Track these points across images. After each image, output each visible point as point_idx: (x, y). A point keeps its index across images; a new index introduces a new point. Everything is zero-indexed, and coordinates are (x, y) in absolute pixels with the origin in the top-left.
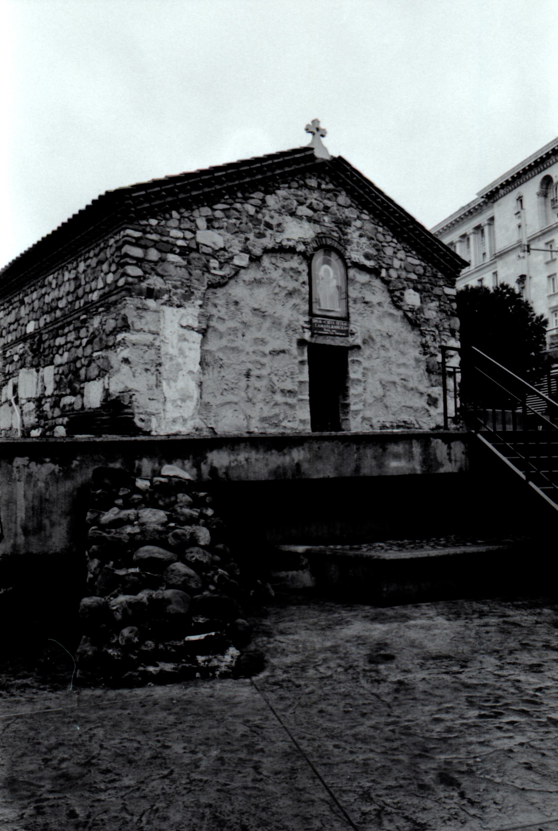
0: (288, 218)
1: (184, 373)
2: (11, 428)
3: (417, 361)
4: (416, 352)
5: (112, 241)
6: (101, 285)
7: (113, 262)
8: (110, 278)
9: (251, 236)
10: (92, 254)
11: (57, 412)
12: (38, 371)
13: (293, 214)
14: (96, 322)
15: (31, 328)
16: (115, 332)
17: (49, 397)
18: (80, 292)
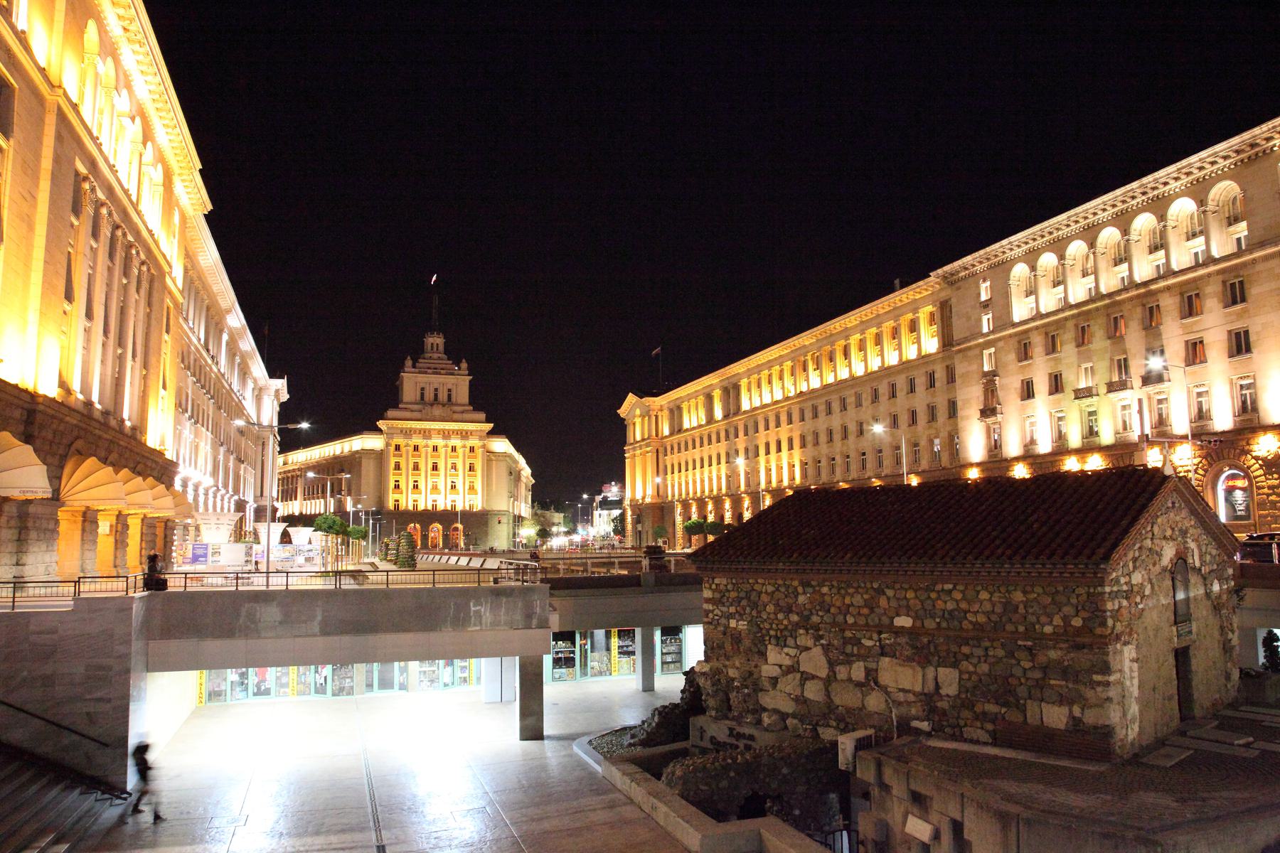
0: (1164, 543)
1: (1133, 700)
2: (861, 709)
3: (1219, 641)
4: (1216, 633)
5: (1081, 590)
6: (1057, 620)
7: (1084, 609)
8: (1077, 622)
9: (1151, 566)
10: (1039, 590)
11: (966, 714)
12: (923, 668)
13: (1165, 538)
14: (1053, 654)
15: (904, 621)
16: (1093, 670)
17: (948, 696)
18: (1015, 617)
